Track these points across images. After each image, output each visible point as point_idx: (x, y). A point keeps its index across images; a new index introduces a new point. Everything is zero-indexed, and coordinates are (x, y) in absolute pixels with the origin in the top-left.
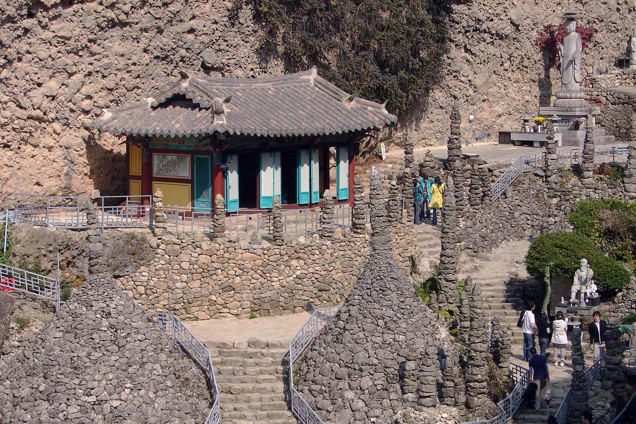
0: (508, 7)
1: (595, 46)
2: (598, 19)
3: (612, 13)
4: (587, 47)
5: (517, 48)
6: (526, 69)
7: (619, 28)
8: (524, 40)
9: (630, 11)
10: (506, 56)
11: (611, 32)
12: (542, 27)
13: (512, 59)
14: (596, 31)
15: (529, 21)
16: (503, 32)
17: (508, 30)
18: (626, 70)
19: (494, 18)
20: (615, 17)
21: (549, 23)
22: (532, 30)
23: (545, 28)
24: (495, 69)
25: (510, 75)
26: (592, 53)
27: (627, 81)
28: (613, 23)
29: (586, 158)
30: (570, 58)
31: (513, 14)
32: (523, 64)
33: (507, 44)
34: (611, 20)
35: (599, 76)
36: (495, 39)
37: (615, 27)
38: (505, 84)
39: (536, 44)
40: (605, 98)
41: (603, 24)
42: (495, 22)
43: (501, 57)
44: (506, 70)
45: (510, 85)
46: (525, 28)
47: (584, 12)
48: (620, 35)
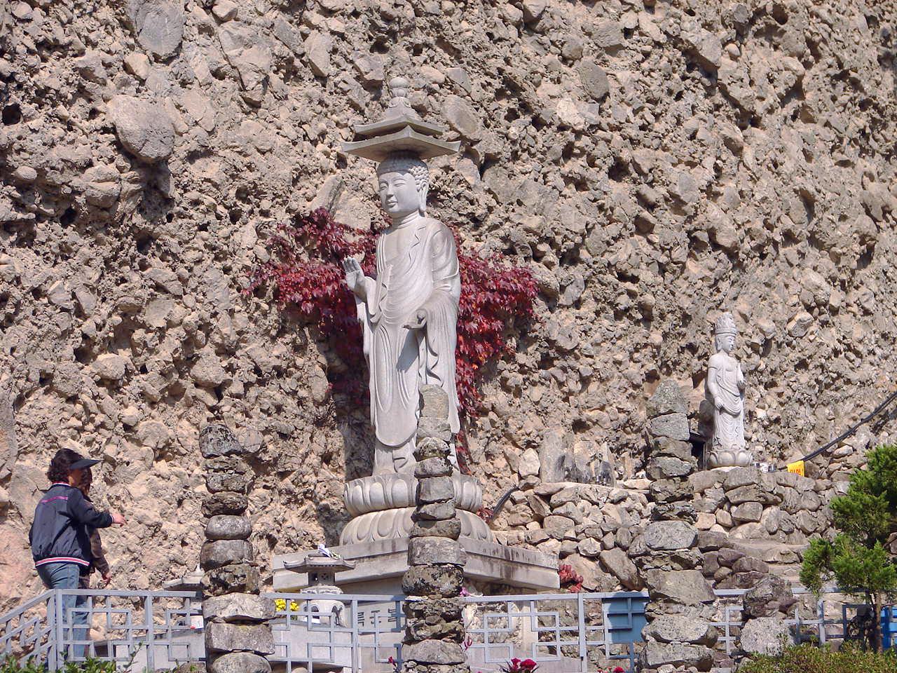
0: (101, 72)
1: (546, 362)
2: (552, 243)
3: (614, 229)
4: (510, 358)
5: (159, 288)
6: (211, 401)
7: (649, 298)
8: (191, 255)
9: (695, 245)
10: (101, 315)
11: (618, 315)
12: (286, 219)
13: (138, 334)
14: (550, 297)
15: (212, 169)
16: (76, 182)
17: (104, 178)
19: (27, 108)
20: (627, 251)
21: (314, 206)
22: (235, 217)
23: (299, 220)
24: (48, 366)
25: (131, 412)
26: (536, 393)
28: (623, 277)
29: (420, 614)
30: (410, 319)
31: (123, 110)
32: (198, 370)
33: (106, 251)
34: (611, 258)
35: (570, 485)
36: (40, 217)
37: (632, 294)
38: (110, 451)
39: (259, 291)
40: (593, 565)
41: (578, 272)
42: (33, 124)
43: (79, 312)
44: (112, 385)
45: (136, 464)
46: (193, 195)
47: (484, 199)
48: (656, 338)
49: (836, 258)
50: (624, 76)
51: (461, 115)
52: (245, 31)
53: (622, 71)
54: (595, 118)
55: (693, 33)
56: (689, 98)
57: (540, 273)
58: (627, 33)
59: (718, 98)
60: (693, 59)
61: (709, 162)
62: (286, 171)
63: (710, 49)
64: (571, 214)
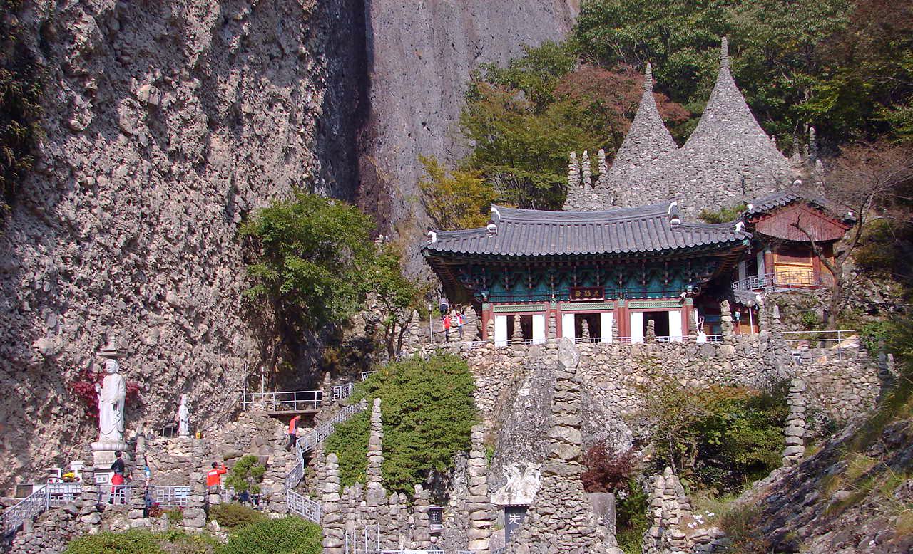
18: (174, 440)
24: (16, 409)
27: (175, 451)
28: (160, 385)
49: (212, 379)
51: (123, 342)
52: (71, 321)
53: (163, 330)
55: (183, 320)
56: (179, 337)
57: (141, 384)
60: (182, 327)
61: (183, 354)
62: (79, 358)
64: (147, 369)
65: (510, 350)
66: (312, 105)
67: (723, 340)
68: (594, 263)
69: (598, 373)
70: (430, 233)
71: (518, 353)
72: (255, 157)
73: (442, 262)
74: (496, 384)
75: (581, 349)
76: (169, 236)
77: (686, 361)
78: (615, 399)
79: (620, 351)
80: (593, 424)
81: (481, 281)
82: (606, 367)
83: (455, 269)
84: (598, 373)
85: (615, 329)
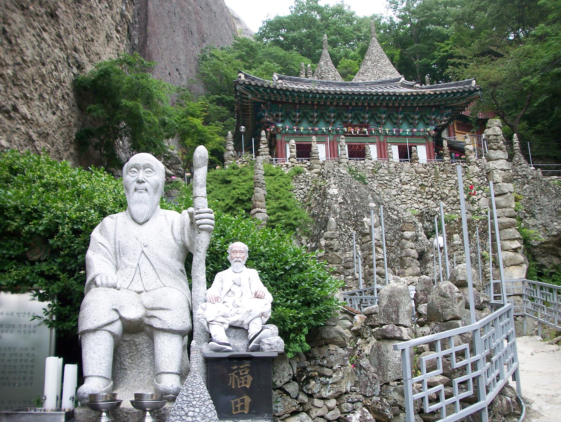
50: (16, 138)
54: (9, 146)
55: (31, 133)
58: (17, 129)
59: (34, 149)
63: (35, 136)
65: (309, 164)
66: (127, 13)
67: (469, 162)
68: (366, 104)
69: (381, 182)
70: (240, 74)
71: (317, 166)
72: (89, 31)
73: (250, 96)
74: (302, 189)
75: (366, 165)
76: (25, 58)
77: (445, 176)
78: (398, 202)
79: (395, 167)
80: (395, 217)
81: (277, 116)
82: (387, 178)
83: (257, 106)
84: (381, 182)
85: (390, 151)
